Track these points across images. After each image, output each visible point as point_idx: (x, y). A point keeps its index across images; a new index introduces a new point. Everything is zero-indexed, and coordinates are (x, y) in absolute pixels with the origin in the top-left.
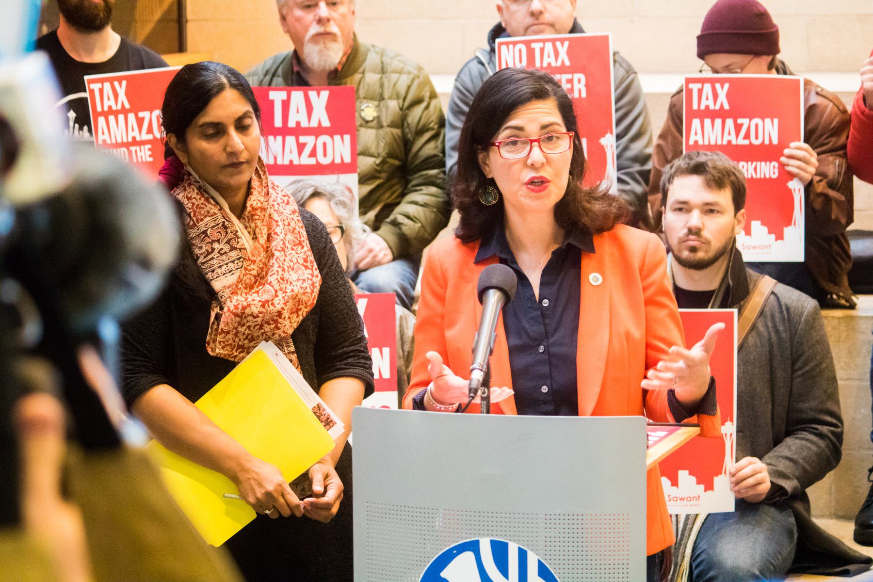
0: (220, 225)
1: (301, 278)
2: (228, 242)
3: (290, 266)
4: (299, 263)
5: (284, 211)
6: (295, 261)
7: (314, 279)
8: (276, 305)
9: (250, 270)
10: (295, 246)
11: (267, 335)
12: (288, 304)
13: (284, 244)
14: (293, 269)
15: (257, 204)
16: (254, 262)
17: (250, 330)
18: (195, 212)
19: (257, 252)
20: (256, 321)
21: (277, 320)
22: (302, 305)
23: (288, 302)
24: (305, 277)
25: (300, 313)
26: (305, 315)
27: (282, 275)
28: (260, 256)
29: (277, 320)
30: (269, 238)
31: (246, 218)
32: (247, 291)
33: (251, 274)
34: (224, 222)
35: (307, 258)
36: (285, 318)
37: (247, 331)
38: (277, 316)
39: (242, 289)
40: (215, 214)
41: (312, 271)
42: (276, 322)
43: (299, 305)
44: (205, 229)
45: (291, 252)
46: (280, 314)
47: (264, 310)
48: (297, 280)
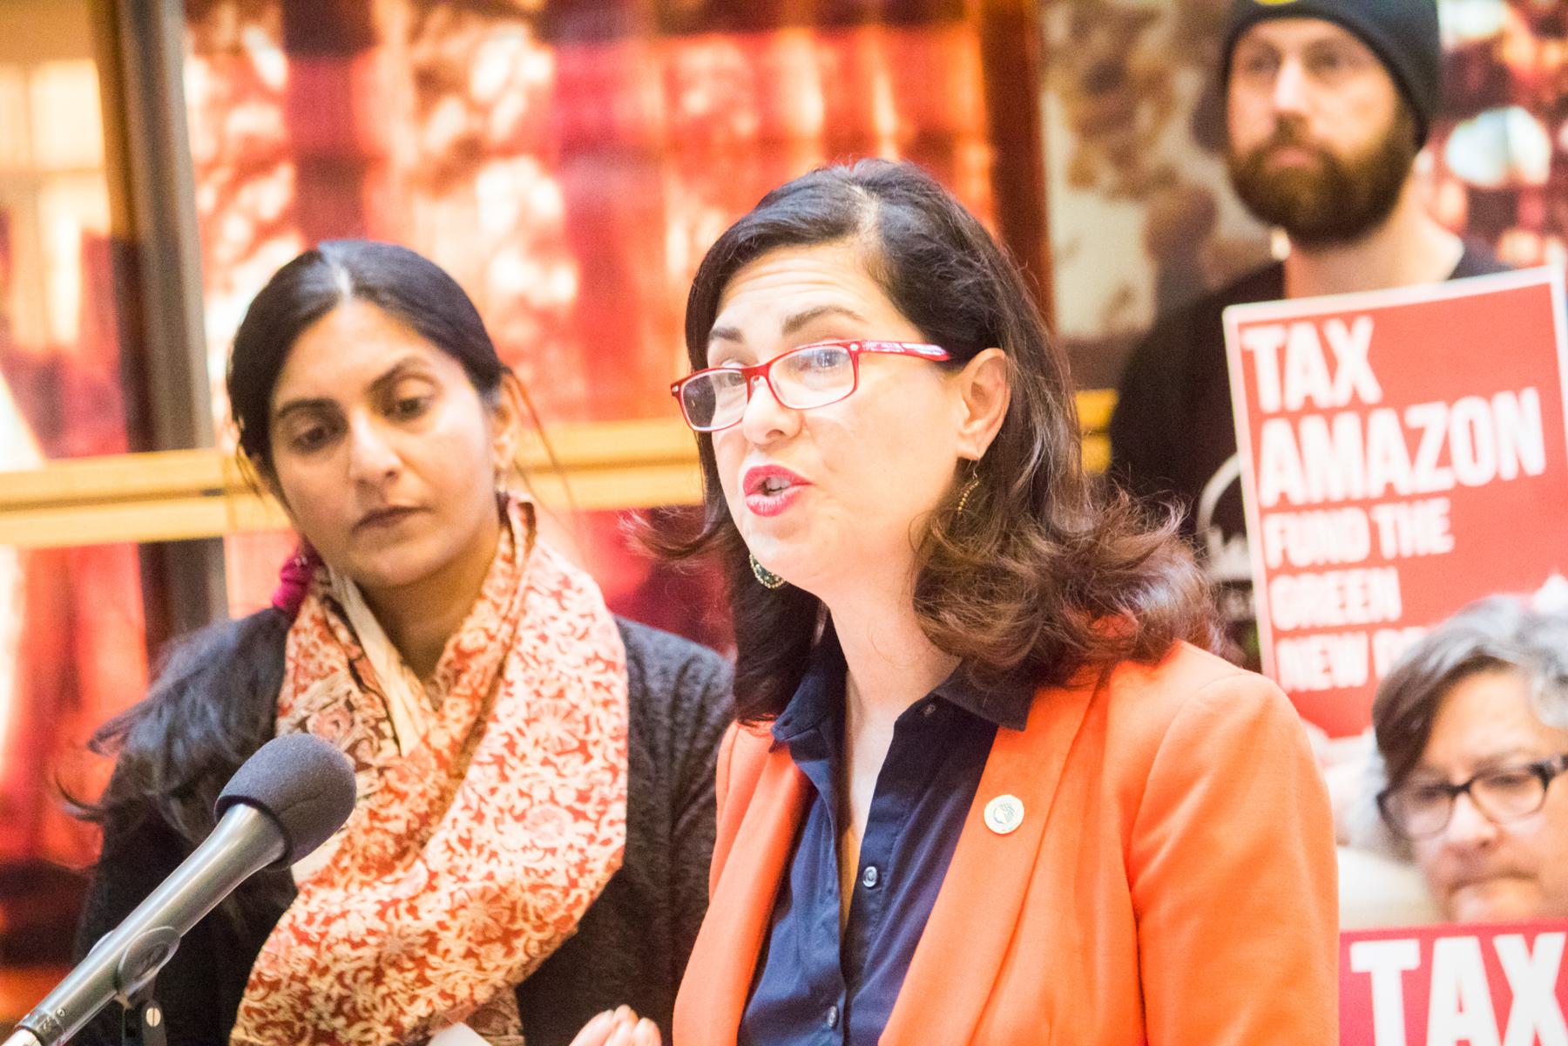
0: (341, 703)
3: (511, 809)
4: (556, 803)
6: (540, 793)
7: (593, 850)
8: (422, 914)
9: (387, 819)
10: (559, 754)
11: (394, 1002)
12: (462, 912)
13: (511, 746)
14: (520, 818)
15: (476, 639)
16: (402, 796)
17: (344, 986)
18: (297, 667)
19: (416, 770)
20: (359, 958)
21: (424, 958)
22: (526, 919)
23: (463, 907)
24: (560, 843)
25: (518, 943)
26: (534, 949)
27: (469, 831)
28: (421, 779)
29: (424, 958)
30: (476, 731)
31: (438, 680)
33: (386, 831)
34: (349, 693)
35: (592, 787)
36: (447, 951)
37: (337, 991)
38: (424, 946)
39: (354, 872)
40: (333, 670)
41: (597, 827)
42: (421, 963)
43: (513, 919)
44: (304, 713)
45: (537, 768)
46: (431, 941)
47: (383, 927)
48: (524, 849)
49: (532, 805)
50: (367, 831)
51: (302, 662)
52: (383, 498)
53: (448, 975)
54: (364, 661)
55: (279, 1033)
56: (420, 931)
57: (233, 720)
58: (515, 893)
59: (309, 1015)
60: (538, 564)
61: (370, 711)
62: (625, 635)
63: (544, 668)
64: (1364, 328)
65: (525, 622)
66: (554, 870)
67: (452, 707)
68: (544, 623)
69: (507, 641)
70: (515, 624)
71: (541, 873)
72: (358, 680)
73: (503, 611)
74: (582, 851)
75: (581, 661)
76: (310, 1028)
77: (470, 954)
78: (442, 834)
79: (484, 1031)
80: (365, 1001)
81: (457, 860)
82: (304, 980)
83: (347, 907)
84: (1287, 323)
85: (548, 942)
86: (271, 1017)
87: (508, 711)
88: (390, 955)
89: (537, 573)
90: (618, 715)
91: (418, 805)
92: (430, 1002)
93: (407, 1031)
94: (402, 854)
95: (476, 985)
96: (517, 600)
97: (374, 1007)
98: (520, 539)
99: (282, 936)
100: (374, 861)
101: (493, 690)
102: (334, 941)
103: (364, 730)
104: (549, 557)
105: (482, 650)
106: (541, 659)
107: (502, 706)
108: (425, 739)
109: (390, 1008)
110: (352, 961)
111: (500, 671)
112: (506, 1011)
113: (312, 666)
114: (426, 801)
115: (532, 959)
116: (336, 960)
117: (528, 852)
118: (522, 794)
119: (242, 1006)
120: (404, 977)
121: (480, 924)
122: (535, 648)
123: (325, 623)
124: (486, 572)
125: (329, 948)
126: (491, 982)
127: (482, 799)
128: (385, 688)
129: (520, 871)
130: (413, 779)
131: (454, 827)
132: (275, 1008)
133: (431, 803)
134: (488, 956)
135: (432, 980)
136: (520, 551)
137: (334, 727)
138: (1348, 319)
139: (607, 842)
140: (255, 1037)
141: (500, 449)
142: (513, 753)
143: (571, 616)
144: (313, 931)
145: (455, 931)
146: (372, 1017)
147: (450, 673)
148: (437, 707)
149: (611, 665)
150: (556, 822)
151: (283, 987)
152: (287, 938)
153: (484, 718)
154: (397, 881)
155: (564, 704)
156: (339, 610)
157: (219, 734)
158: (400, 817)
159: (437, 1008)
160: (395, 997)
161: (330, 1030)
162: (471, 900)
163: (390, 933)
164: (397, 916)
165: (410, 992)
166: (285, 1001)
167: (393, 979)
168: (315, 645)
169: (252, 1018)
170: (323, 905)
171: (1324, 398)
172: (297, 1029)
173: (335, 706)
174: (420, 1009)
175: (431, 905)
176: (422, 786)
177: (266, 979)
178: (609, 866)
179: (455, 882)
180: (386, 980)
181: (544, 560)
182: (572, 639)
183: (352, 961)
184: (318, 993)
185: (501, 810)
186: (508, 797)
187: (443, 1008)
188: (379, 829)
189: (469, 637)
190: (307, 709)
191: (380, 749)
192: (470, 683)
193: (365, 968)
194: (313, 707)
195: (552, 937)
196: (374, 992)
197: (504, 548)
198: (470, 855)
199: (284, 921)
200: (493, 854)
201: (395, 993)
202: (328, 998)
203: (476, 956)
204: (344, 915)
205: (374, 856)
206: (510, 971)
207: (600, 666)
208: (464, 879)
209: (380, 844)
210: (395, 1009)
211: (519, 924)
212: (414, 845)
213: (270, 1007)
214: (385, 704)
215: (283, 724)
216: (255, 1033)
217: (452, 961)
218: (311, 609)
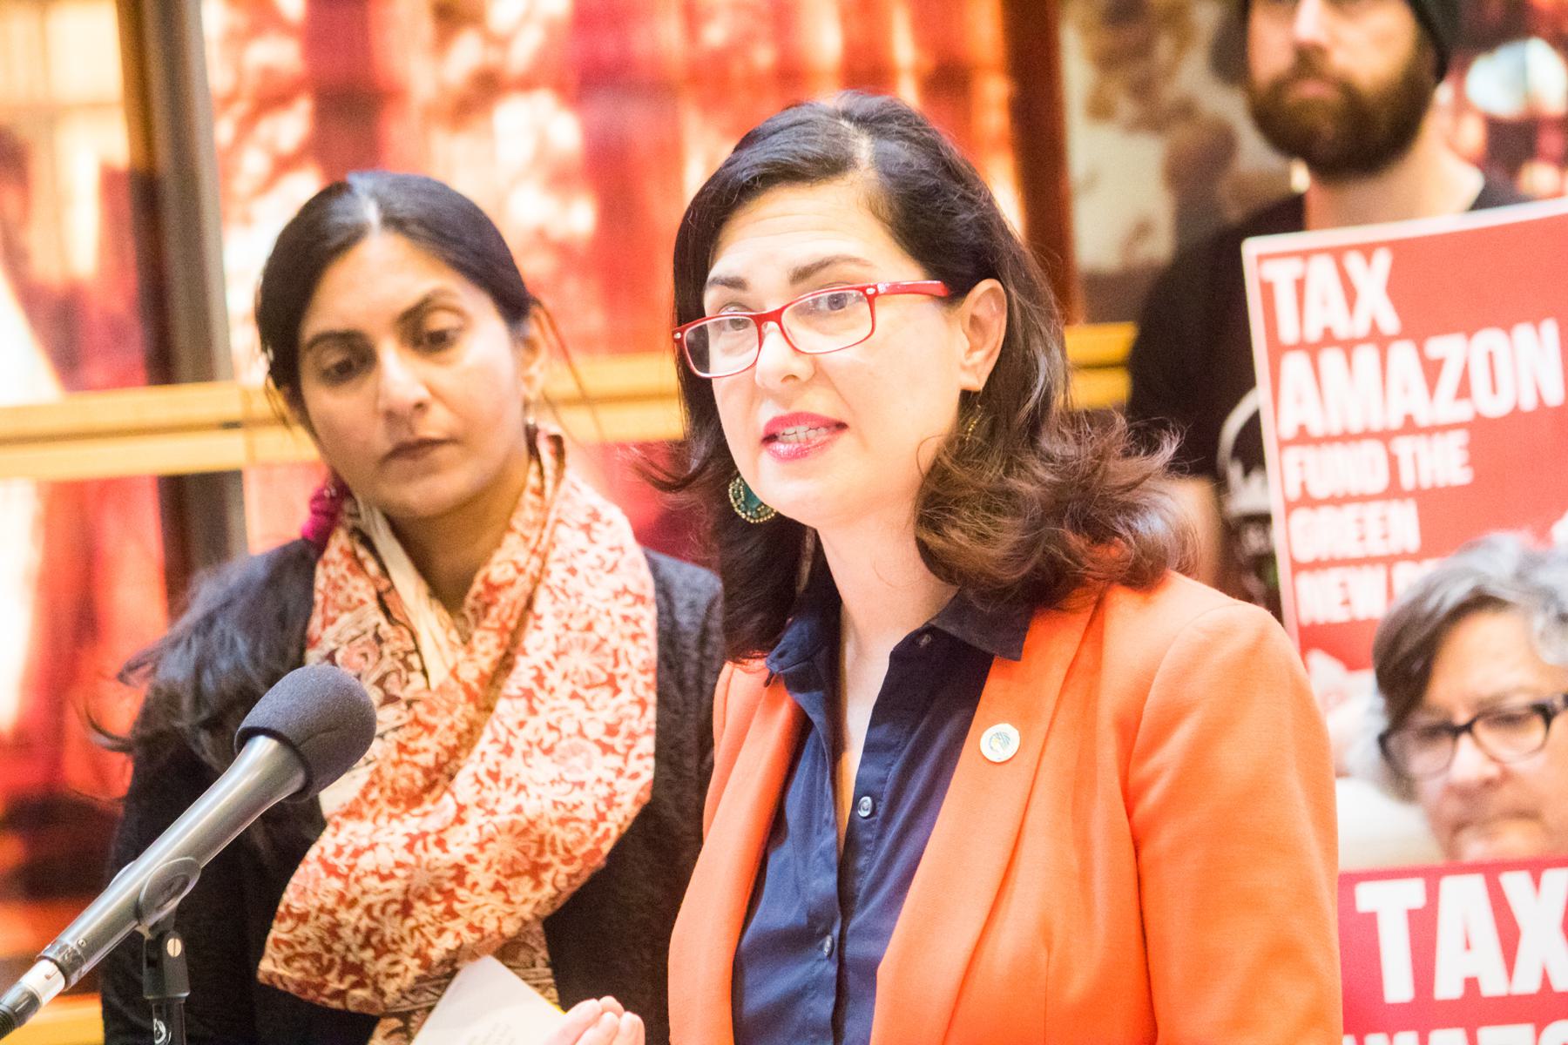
0: (370, 635)
1: (569, 777)
2: (380, 682)
3: (540, 743)
5: (587, 591)
6: (568, 727)
7: (621, 784)
8: (450, 846)
9: (416, 752)
10: (588, 687)
11: (423, 935)
12: (490, 846)
13: (540, 679)
14: (548, 751)
15: (505, 571)
16: (430, 729)
18: (326, 599)
19: (444, 703)
20: (388, 891)
21: (452, 891)
22: (554, 853)
23: (491, 840)
24: (589, 777)
25: (547, 877)
26: (562, 882)
27: (498, 764)
28: (450, 712)
29: (452, 891)
30: (505, 664)
31: (467, 613)
32: (395, 811)
33: (415, 764)
34: (377, 626)
35: (621, 721)
36: (475, 885)
37: (365, 923)
38: (453, 879)
39: (382, 804)
40: (362, 602)
41: (626, 761)
42: (449, 895)
43: (541, 853)
44: (333, 645)
46: (460, 874)
47: (411, 859)
48: (553, 782)
49: (561, 738)
50: (396, 764)
51: (331, 594)
52: (411, 430)
53: (476, 908)
54: (393, 594)
55: (307, 964)
56: (448, 865)
57: (262, 653)
58: (544, 827)
59: (338, 947)
60: (567, 497)
61: (398, 644)
62: (654, 568)
63: (573, 601)
64: (1383, 260)
65: (553, 555)
66: (582, 803)
67: (481, 640)
68: (573, 556)
69: (536, 574)
70: (544, 557)
71: (570, 806)
72: (387, 613)
73: (532, 544)
74: (610, 784)
75: (609, 594)
76: (338, 960)
77: (498, 887)
78: (471, 767)
79: (512, 964)
80: (393, 934)
81: (485, 793)
82: (332, 912)
83: (375, 840)
84: (1305, 255)
85: (576, 875)
86: (299, 949)
87: (537, 644)
88: (418, 888)
89: (566, 506)
90: (647, 648)
91: (447, 739)
92: (458, 935)
93: (435, 964)
94: (430, 787)
95: (504, 917)
96: (546, 533)
97: (403, 939)
98: (549, 472)
99: (310, 868)
100: (402, 794)
101: (522, 623)
102: (362, 873)
103: (392, 663)
104: (578, 490)
105: (511, 583)
106: (569, 591)
107: (531, 639)
108: (454, 673)
109: (418, 940)
110: (381, 893)
111: (530, 603)
112: (534, 944)
113: (341, 599)
114: (455, 733)
115: (560, 892)
116: (364, 892)
117: (556, 785)
118: (551, 727)
119: (270, 938)
120: (433, 910)
121: (508, 857)
122: (564, 581)
123: (354, 555)
124: (515, 504)
125: (357, 880)
126: (519, 915)
127: (510, 732)
128: (414, 621)
129: (548, 804)
130: (442, 712)
131: (482, 760)
132: (303, 940)
133: (459, 736)
134: (516, 889)
135: (460, 913)
136: (549, 483)
137: (363, 660)
138: (1367, 250)
139: (635, 776)
140: (285, 969)
141: (529, 380)
142: (541, 686)
143: (601, 549)
144: (341, 863)
145: (483, 864)
146: (400, 950)
147: (479, 605)
148: (466, 640)
149: (640, 599)
150: (584, 755)
151: (311, 919)
152: (315, 870)
153: (512, 651)
154: (425, 814)
155: (593, 638)
156: (367, 542)
157: (249, 668)
158: (428, 750)
159: (465, 941)
160: (424, 930)
161: (358, 963)
162: (499, 832)
163: (418, 866)
164: (425, 848)
165: (438, 924)
166: (316, 936)
167: (421, 911)
168: (344, 577)
169: (282, 951)
170: (352, 838)
171: (1342, 330)
172: (325, 962)
173: (364, 638)
174: (448, 942)
175: (459, 839)
176: (451, 719)
177: (294, 911)
178: (637, 801)
179: (483, 816)
180: (414, 912)
181: (573, 492)
182: (601, 573)
183: (381, 893)
184: (346, 926)
185: (530, 744)
186: (537, 730)
187: (471, 941)
188: (407, 762)
189: (498, 569)
190: (335, 641)
191: (408, 682)
192: (499, 616)
193: (394, 901)
194: (342, 639)
195: (581, 870)
196: (402, 924)
197: (533, 480)
198: (498, 788)
199: (313, 853)
200: (521, 788)
201: (423, 926)
202: (356, 930)
203: (505, 889)
204: (372, 847)
205: (402, 790)
206: (538, 904)
207: (629, 599)
208: (493, 813)
209: (408, 777)
210: (423, 942)
211: (548, 858)
212: (442, 778)
213: (299, 939)
214: (414, 636)
215: (313, 656)
216: (283, 964)
217: (480, 894)
218: (339, 542)
